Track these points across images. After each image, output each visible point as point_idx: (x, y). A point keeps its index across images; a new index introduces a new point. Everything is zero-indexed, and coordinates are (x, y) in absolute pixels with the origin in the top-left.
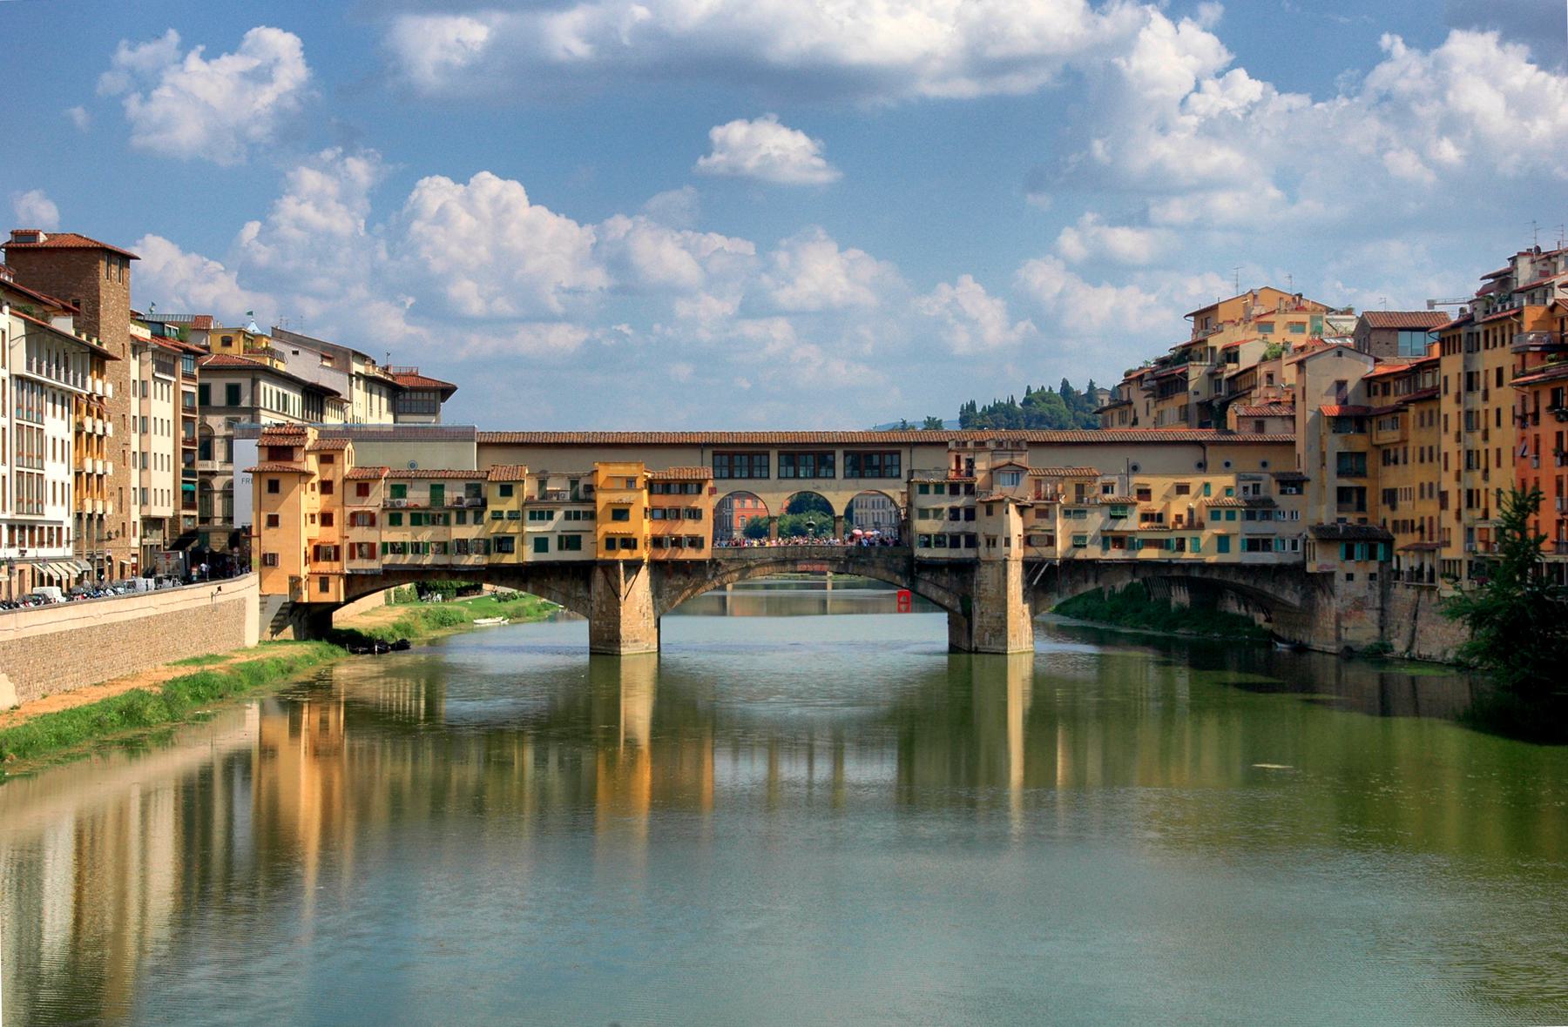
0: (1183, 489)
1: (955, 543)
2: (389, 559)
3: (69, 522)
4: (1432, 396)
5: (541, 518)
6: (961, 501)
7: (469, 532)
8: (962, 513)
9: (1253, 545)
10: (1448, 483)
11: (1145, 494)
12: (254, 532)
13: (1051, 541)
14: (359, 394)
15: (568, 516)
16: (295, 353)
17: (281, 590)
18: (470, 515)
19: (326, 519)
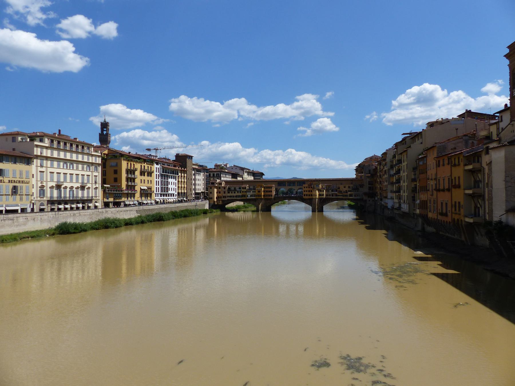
0: (345, 187)
1: (309, 195)
2: (229, 198)
3: (176, 193)
4: (377, 172)
5: (249, 192)
6: (310, 189)
7: (240, 194)
8: (310, 191)
9: (355, 196)
10: (378, 186)
11: (339, 188)
12: (209, 194)
13: (323, 195)
14: (246, 174)
15: (253, 192)
16: (236, 169)
17: (212, 203)
18: (239, 192)
19: (220, 193)
